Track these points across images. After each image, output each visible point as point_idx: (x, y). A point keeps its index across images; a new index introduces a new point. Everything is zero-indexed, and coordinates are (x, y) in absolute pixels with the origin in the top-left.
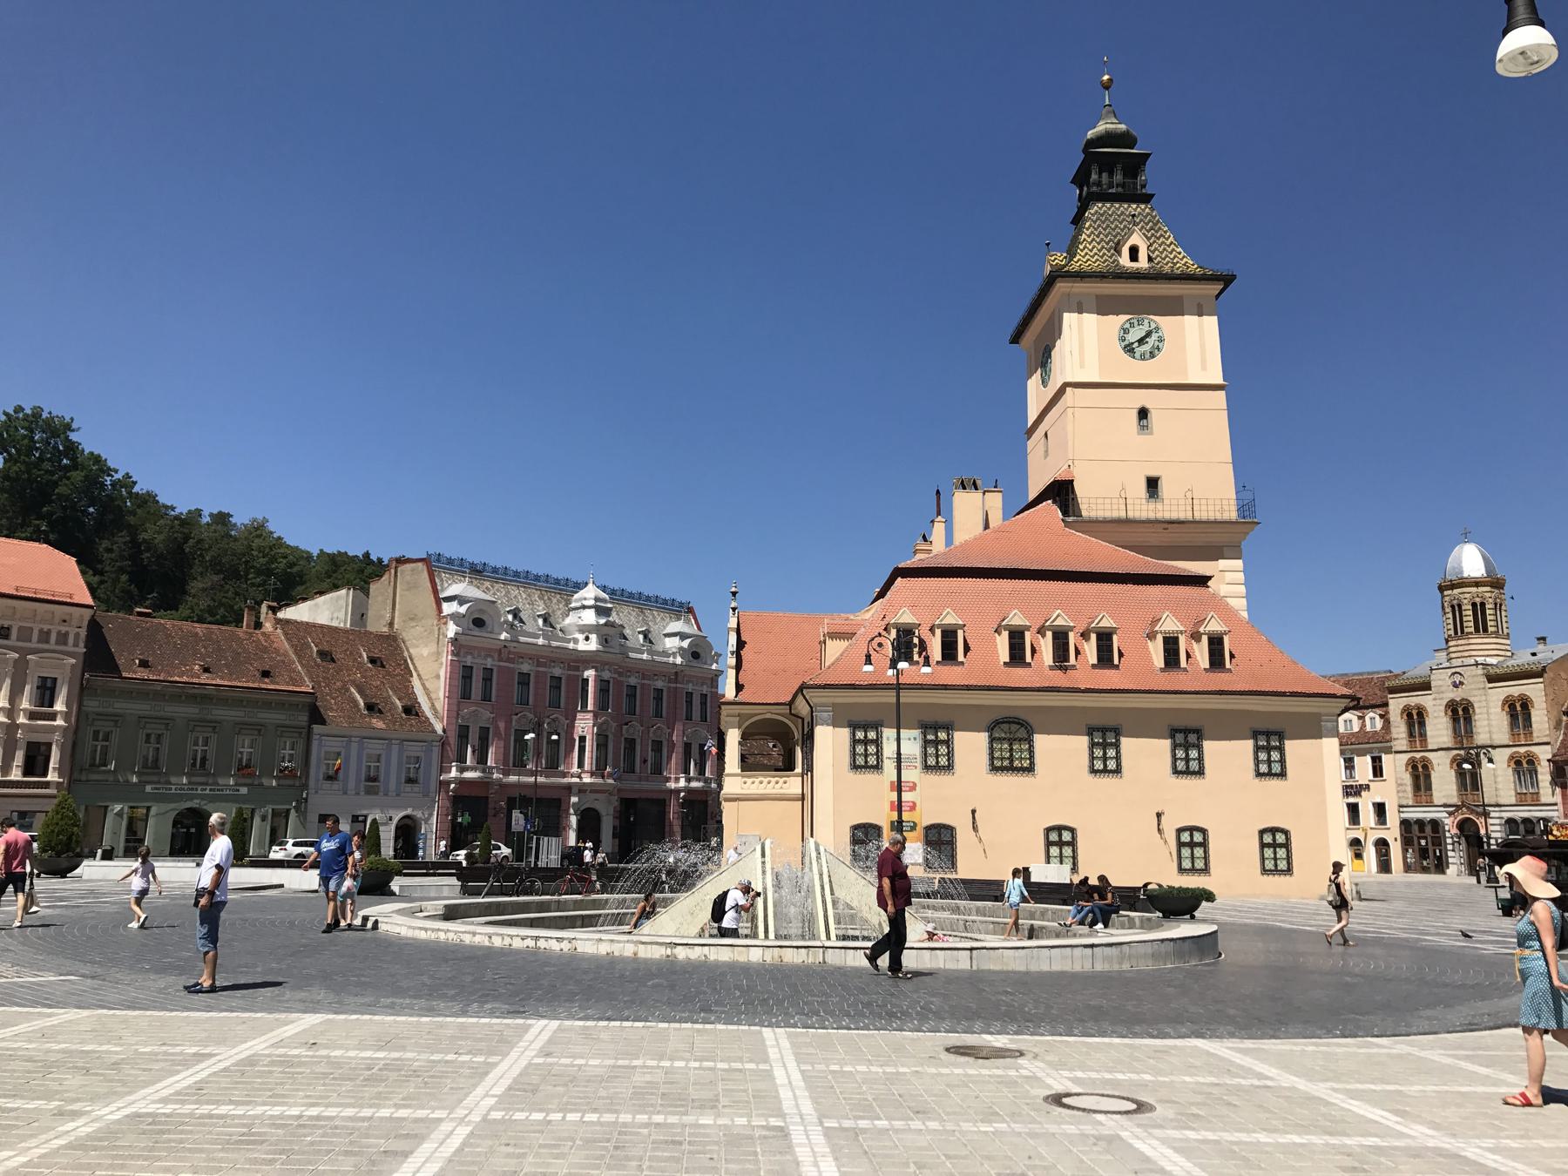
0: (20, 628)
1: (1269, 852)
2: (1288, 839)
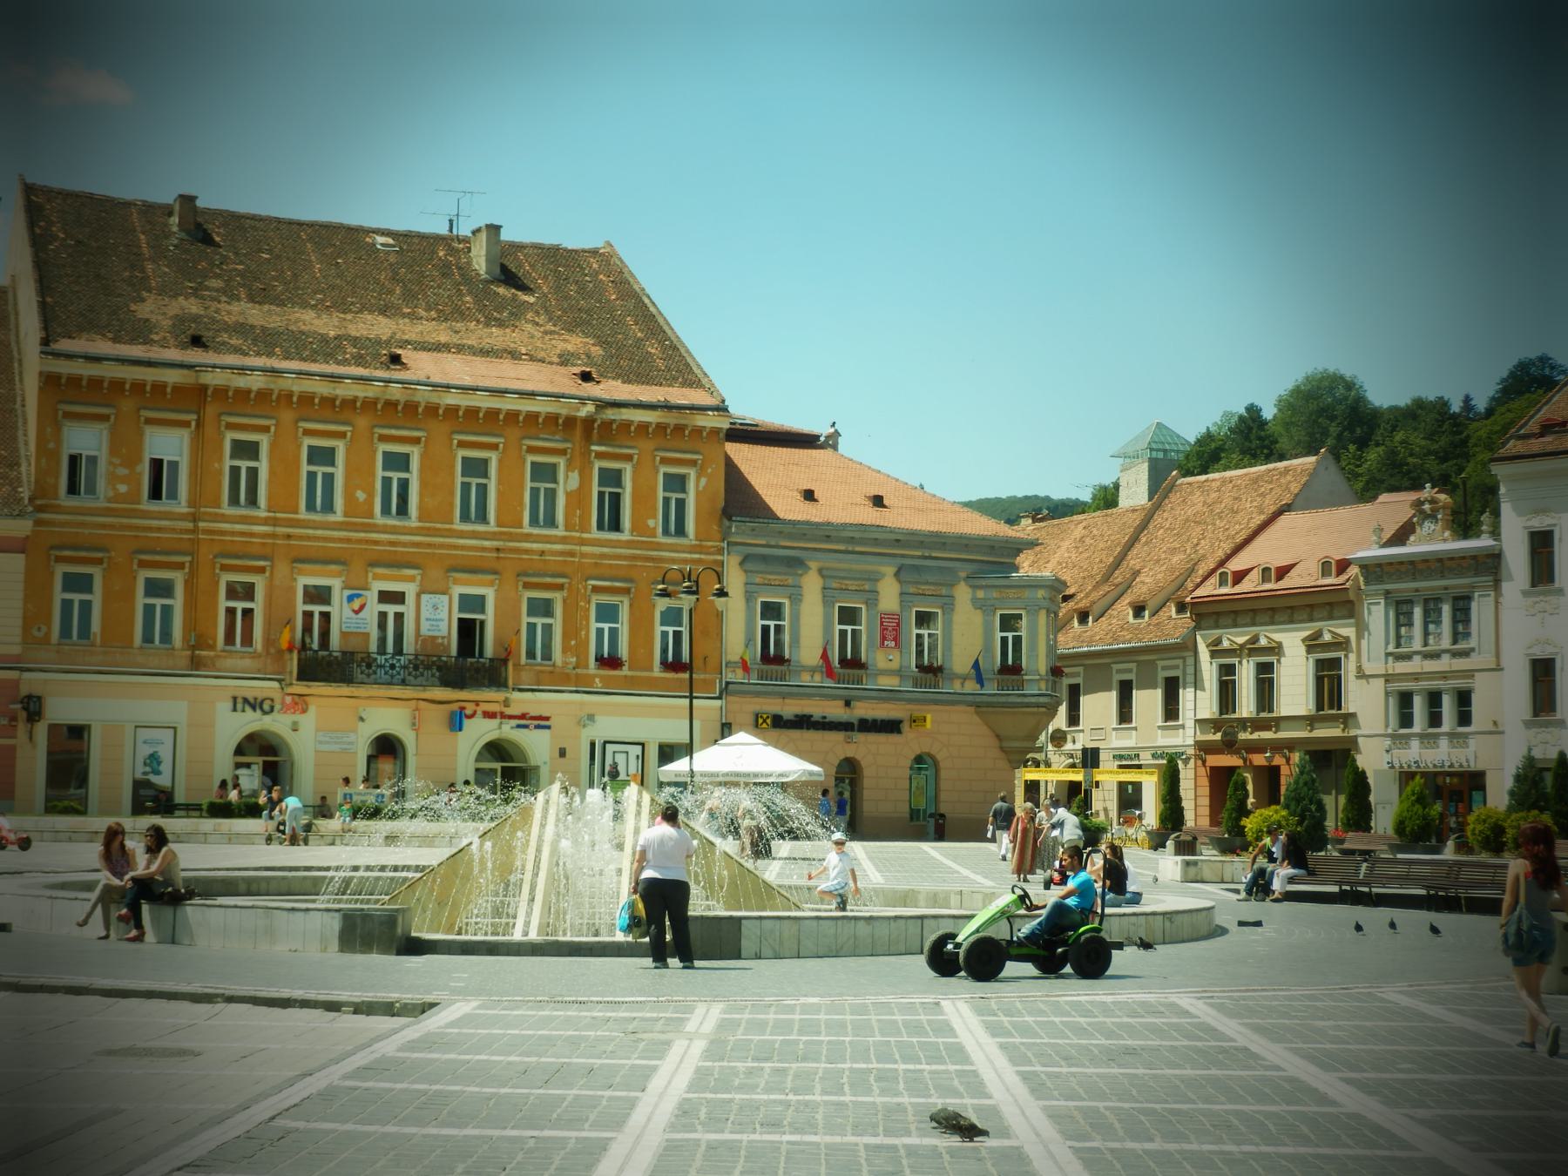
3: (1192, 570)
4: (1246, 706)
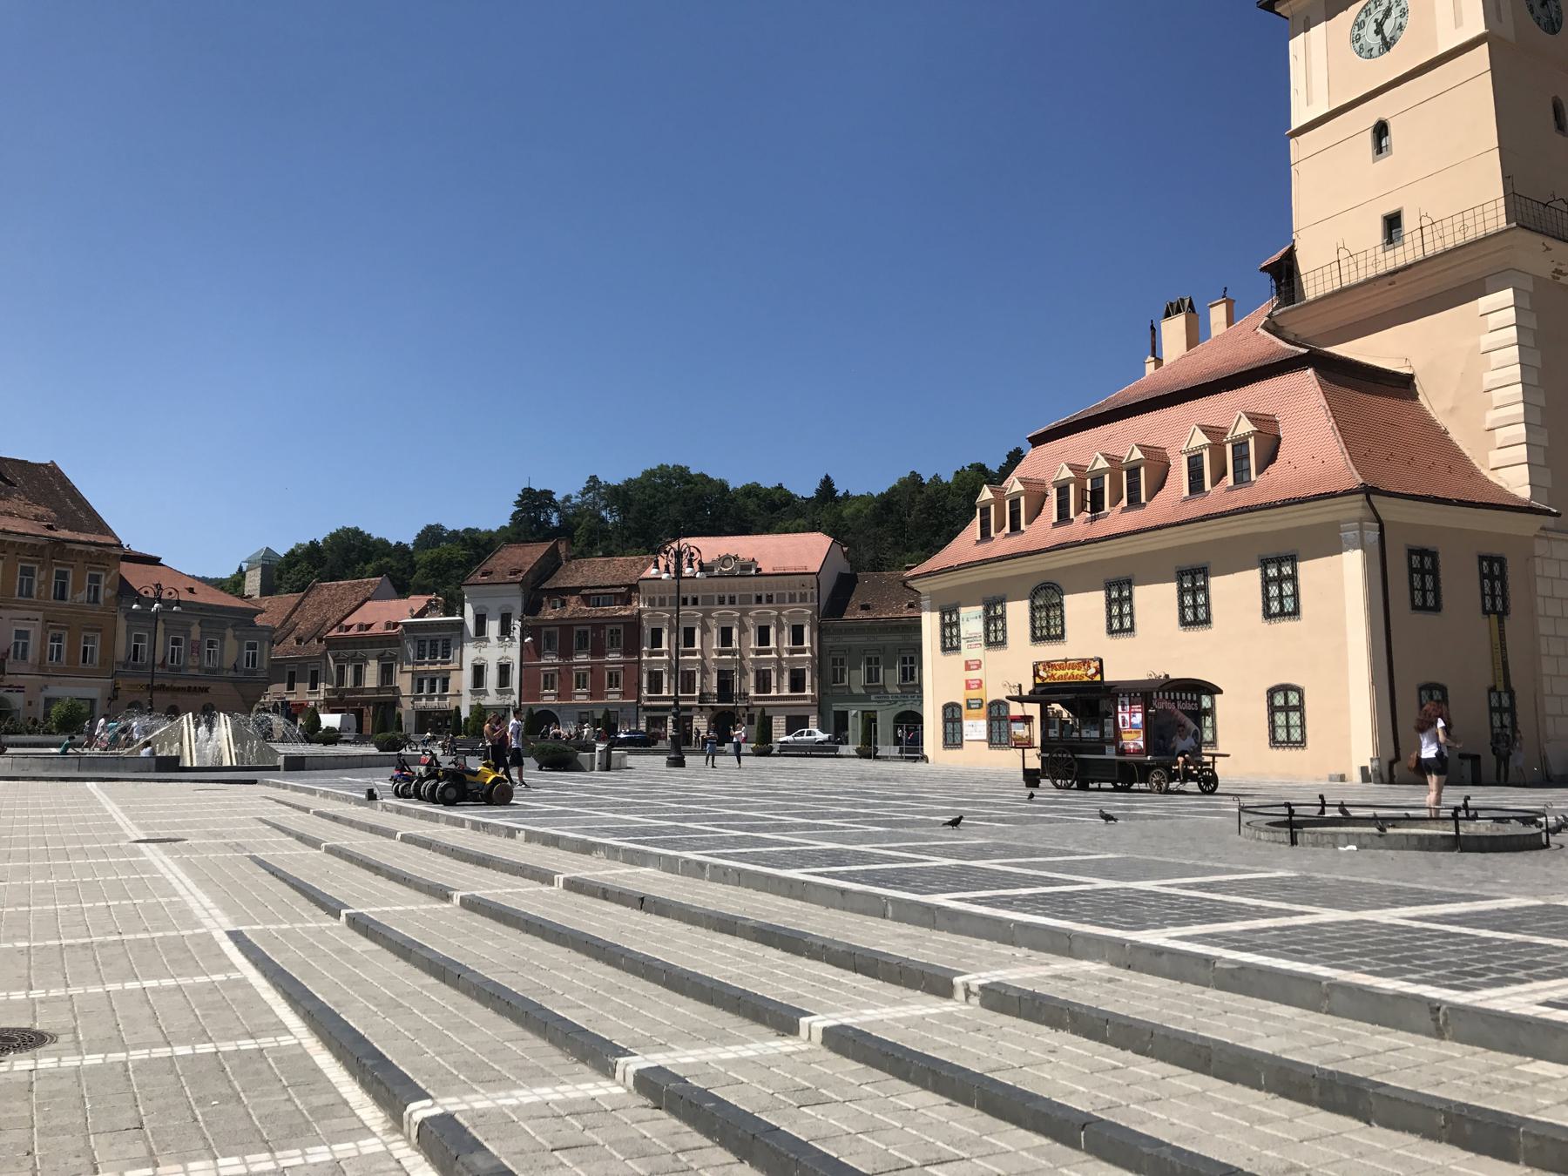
0: (741, 596)
1: (1280, 718)
2: (1301, 699)
3: (325, 624)
4: (349, 684)
